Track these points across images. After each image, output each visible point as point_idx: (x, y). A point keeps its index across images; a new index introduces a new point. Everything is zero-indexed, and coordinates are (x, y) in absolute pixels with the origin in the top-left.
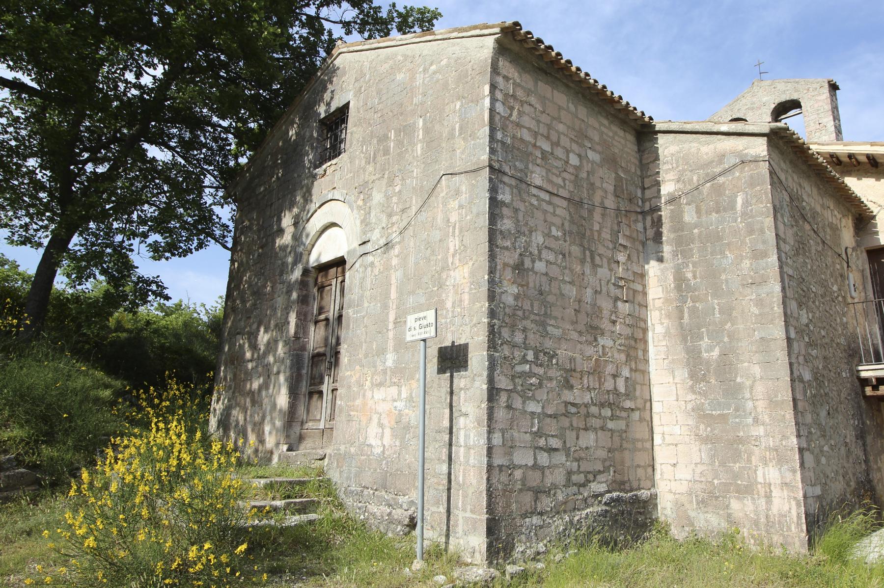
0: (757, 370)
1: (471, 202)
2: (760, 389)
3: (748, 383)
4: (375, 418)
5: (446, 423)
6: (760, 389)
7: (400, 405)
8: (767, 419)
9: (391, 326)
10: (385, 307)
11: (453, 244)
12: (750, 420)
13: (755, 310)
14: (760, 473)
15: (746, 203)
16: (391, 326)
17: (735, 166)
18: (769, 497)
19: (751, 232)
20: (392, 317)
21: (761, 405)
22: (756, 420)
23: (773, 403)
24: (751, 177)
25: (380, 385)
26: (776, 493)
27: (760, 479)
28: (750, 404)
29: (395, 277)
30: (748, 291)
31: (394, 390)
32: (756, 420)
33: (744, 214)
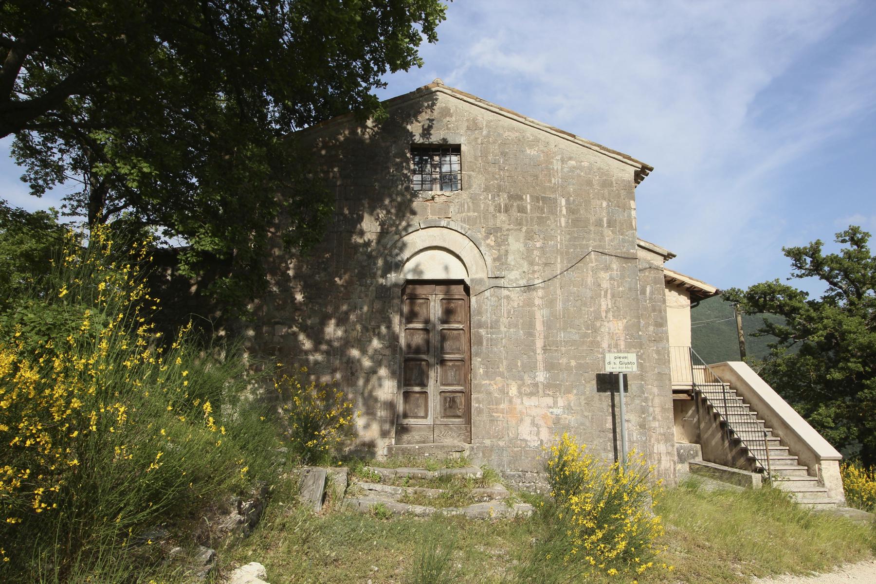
0: (655, 390)
1: (622, 277)
2: (657, 401)
3: (651, 397)
4: (528, 420)
5: (609, 425)
6: (657, 401)
7: (556, 411)
8: (660, 418)
9: (539, 351)
10: (530, 334)
11: (605, 303)
12: (651, 418)
13: (655, 355)
14: (655, 448)
15: (652, 293)
16: (539, 351)
17: (646, 269)
18: (659, 461)
19: (654, 310)
20: (539, 344)
21: (657, 410)
22: (654, 419)
23: (664, 410)
24: (655, 278)
25: (531, 394)
26: (663, 458)
27: (655, 451)
28: (651, 409)
29: (540, 316)
30: (652, 344)
31: (549, 401)
32: (654, 419)
33: (650, 299)
